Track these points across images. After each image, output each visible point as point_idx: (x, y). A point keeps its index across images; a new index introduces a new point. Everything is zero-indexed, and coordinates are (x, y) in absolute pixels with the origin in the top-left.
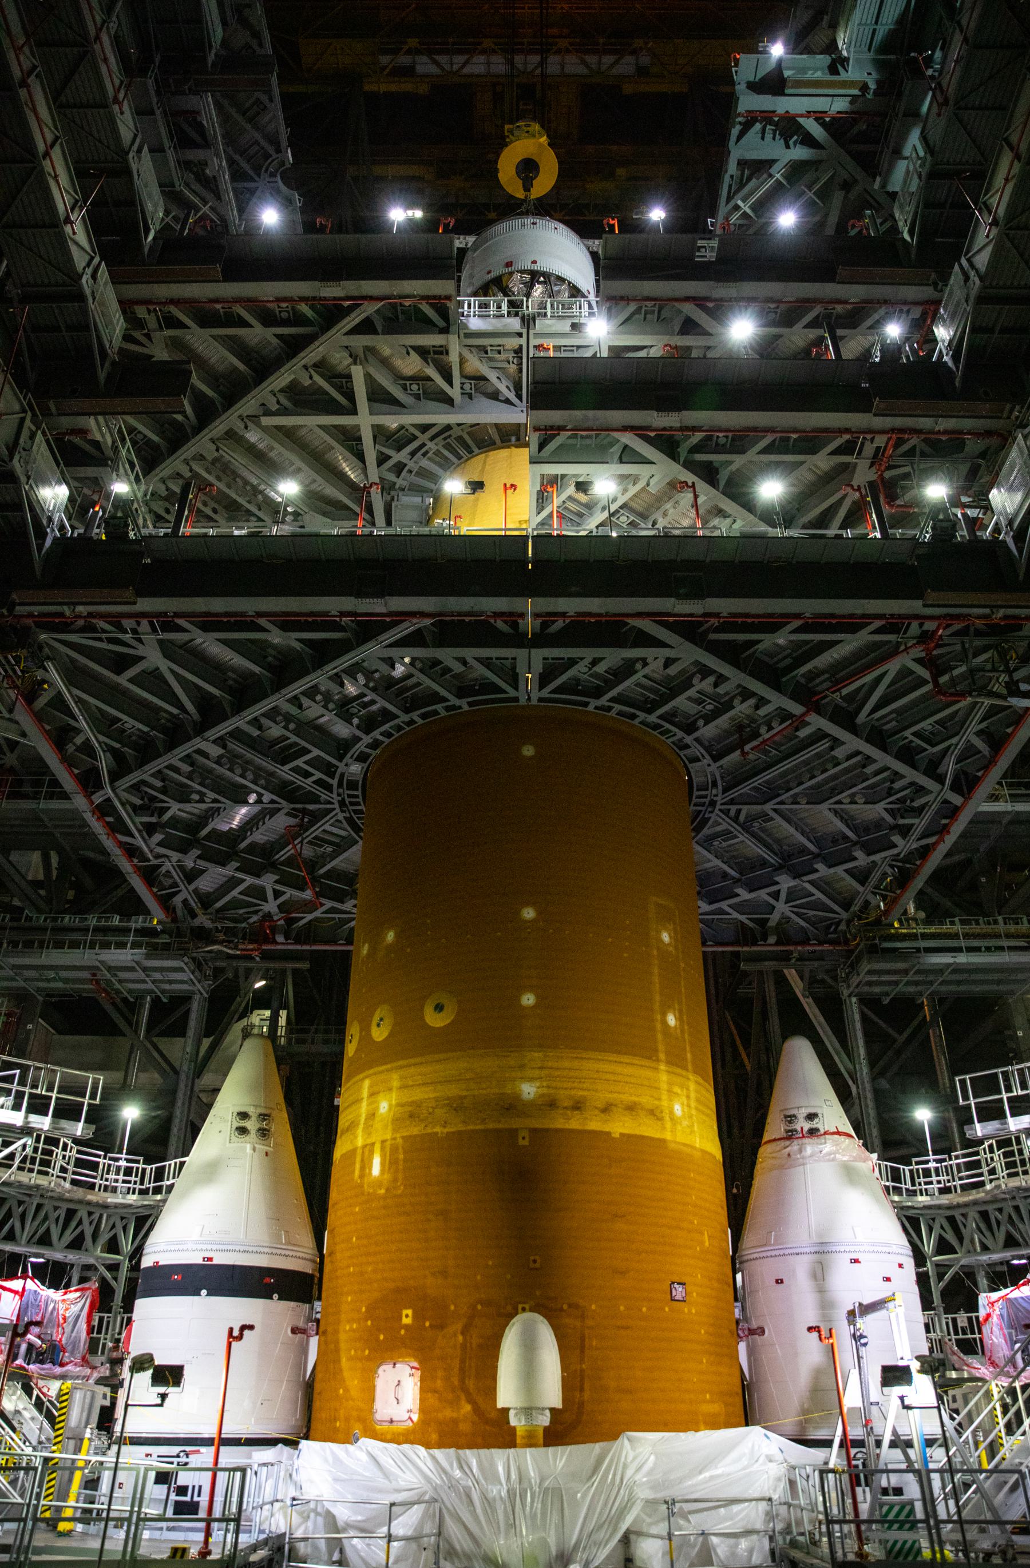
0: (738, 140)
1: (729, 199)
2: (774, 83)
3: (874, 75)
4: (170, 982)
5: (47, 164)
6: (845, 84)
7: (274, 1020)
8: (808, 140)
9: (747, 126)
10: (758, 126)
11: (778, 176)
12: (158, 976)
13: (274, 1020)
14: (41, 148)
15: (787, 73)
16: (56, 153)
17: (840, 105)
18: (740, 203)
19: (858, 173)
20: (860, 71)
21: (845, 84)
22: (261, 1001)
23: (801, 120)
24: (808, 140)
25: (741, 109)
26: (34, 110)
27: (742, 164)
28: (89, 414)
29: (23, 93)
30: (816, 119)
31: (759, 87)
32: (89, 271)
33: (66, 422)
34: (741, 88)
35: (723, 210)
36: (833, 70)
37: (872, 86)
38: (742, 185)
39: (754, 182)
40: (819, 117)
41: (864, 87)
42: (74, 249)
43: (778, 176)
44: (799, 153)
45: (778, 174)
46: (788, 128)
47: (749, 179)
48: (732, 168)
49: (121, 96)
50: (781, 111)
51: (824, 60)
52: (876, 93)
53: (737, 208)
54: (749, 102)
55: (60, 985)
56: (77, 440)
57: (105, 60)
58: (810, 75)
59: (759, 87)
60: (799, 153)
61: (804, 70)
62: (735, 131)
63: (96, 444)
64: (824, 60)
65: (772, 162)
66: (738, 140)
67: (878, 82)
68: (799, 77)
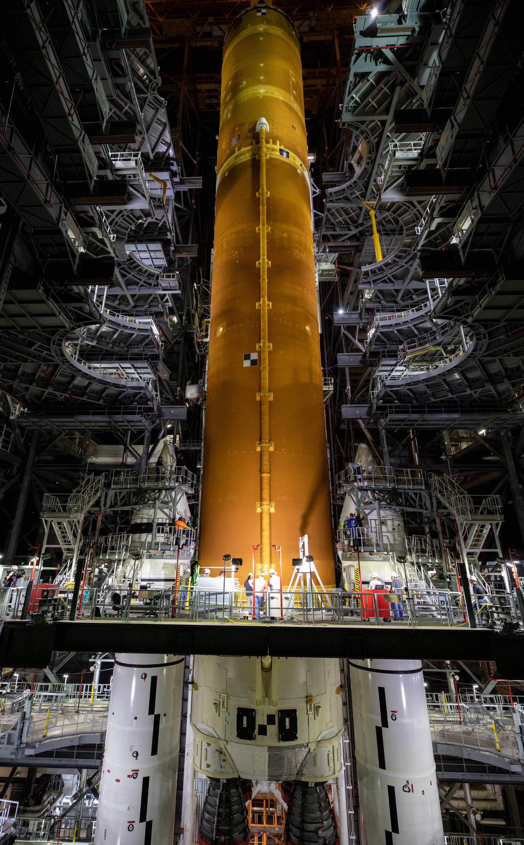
0: (355, 61)
1: (350, 93)
2: (371, 32)
3: (418, 24)
4: (137, 426)
5: (57, 87)
6: (405, 29)
7: (174, 439)
8: (386, 61)
9: (359, 55)
10: (364, 55)
11: (371, 80)
12: (132, 424)
13: (174, 439)
14: (55, 79)
15: (378, 25)
16: (61, 80)
17: (402, 41)
18: (354, 95)
19: (407, 76)
20: (412, 22)
21: (405, 29)
22: (170, 432)
23: (383, 50)
24: (386, 61)
25: (357, 46)
26: (50, 60)
27: (356, 75)
28: (88, 204)
29: (44, 51)
30: (390, 49)
31: (365, 34)
32: (81, 138)
33: (79, 208)
34: (357, 34)
35: (347, 99)
36: (400, 22)
37: (417, 29)
38: (355, 86)
39: (361, 84)
40: (391, 47)
41: (413, 30)
42: (73, 127)
43: (371, 80)
44: (382, 67)
45: (371, 79)
46: (378, 55)
47: (359, 83)
48: (351, 78)
49: (86, 51)
50: (374, 46)
51: (396, 17)
52: (418, 34)
53: (353, 98)
54: (361, 42)
55: (97, 428)
56: (82, 215)
57: (78, 33)
58: (389, 26)
59: (365, 34)
60: (382, 67)
61: (385, 23)
62: (353, 58)
63: (92, 218)
64: (396, 17)
65: (368, 73)
66: (355, 61)
67: (420, 27)
68: (384, 27)
